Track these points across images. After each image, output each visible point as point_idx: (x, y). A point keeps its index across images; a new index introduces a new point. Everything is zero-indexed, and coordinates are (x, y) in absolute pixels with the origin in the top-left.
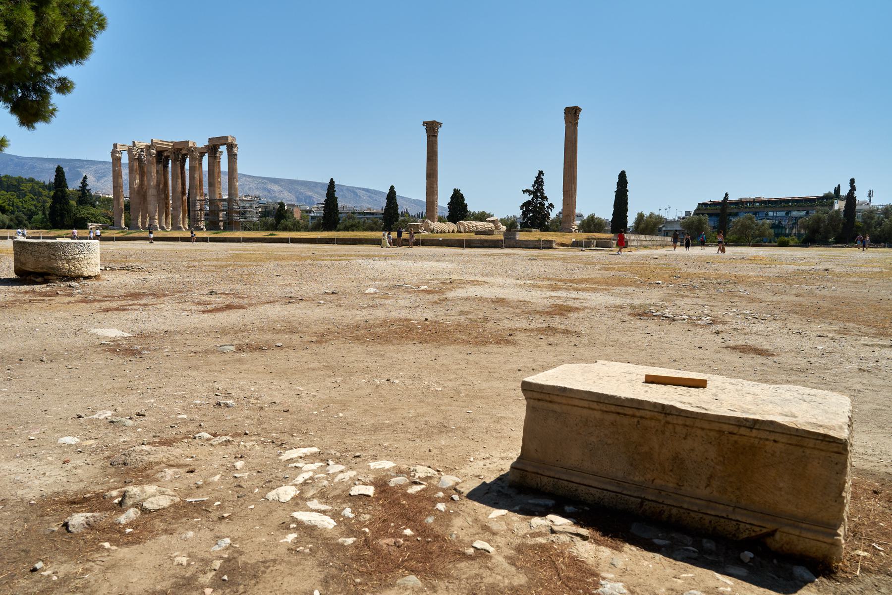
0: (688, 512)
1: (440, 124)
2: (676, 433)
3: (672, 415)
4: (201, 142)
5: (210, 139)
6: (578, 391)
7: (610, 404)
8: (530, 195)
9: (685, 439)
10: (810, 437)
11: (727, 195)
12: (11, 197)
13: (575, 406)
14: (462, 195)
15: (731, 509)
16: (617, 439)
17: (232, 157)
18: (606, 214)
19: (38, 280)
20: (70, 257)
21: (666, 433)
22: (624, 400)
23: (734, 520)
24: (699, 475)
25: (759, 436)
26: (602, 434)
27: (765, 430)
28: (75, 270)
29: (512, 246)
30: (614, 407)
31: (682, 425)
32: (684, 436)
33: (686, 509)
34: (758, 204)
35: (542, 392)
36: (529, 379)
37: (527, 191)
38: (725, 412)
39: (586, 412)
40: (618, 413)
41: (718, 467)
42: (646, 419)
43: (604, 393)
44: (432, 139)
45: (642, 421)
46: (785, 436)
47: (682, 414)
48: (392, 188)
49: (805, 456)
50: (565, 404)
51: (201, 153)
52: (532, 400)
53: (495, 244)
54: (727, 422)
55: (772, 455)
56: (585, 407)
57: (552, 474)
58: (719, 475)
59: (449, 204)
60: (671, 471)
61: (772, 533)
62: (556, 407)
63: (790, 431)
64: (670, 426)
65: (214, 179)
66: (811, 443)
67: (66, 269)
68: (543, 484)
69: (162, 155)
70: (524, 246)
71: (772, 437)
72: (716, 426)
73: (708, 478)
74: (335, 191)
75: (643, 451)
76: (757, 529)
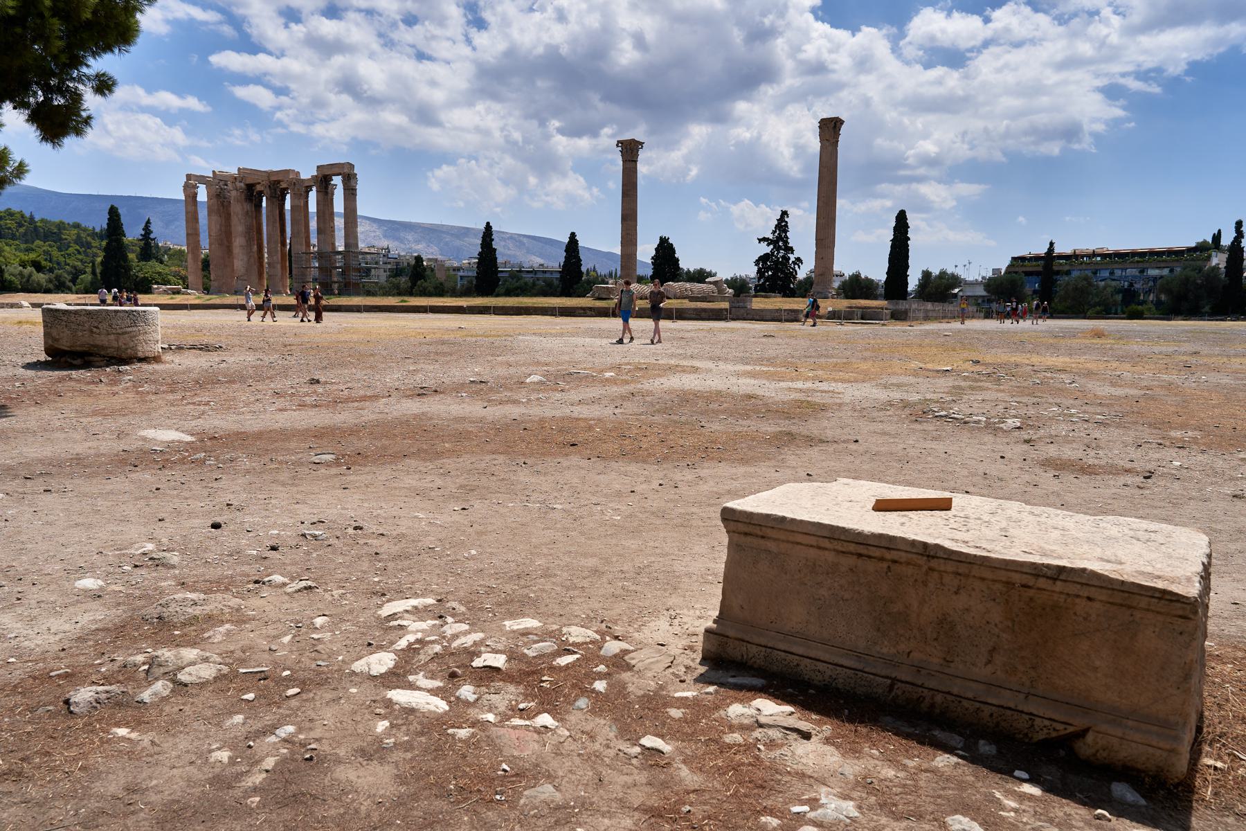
0: (958, 699)
2: (944, 585)
3: (938, 558)
4: (307, 172)
5: (318, 167)
6: (801, 521)
7: (848, 541)
8: (768, 245)
9: (956, 593)
10: (1142, 593)
11: (1052, 244)
12: (50, 249)
13: (798, 543)
15: (1022, 696)
16: (858, 592)
17: (350, 193)
18: (878, 271)
19: (75, 362)
20: (119, 331)
21: (930, 584)
22: (867, 536)
23: (1027, 714)
24: (977, 646)
25: (1065, 592)
26: (836, 584)
27: (1074, 582)
28: (127, 349)
29: (741, 317)
30: (853, 545)
31: (953, 573)
32: (955, 590)
33: (956, 696)
34: (1099, 259)
35: (750, 523)
36: (731, 504)
37: (764, 239)
38: (1017, 554)
39: (813, 553)
40: (860, 555)
41: (1004, 635)
42: (901, 563)
43: (840, 525)
44: (631, 165)
45: (894, 567)
46: (1104, 591)
47: (951, 557)
48: (573, 235)
49: (1133, 621)
50: (783, 541)
51: (307, 187)
52: (736, 535)
53: (717, 315)
54: (1019, 569)
55: (1085, 619)
56: (812, 546)
57: (763, 641)
58: (1006, 647)
59: (653, 258)
60: (936, 639)
61: (1082, 733)
62: (771, 545)
63: (1112, 584)
64: (936, 575)
66: (1144, 602)
67: (112, 347)
68: (751, 655)
69: (253, 191)
70: (758, 317)
71: (1085, 592)
72: (1003, 576)
73: (990, 651)
75: (895, 610)
76: (1060, 727)
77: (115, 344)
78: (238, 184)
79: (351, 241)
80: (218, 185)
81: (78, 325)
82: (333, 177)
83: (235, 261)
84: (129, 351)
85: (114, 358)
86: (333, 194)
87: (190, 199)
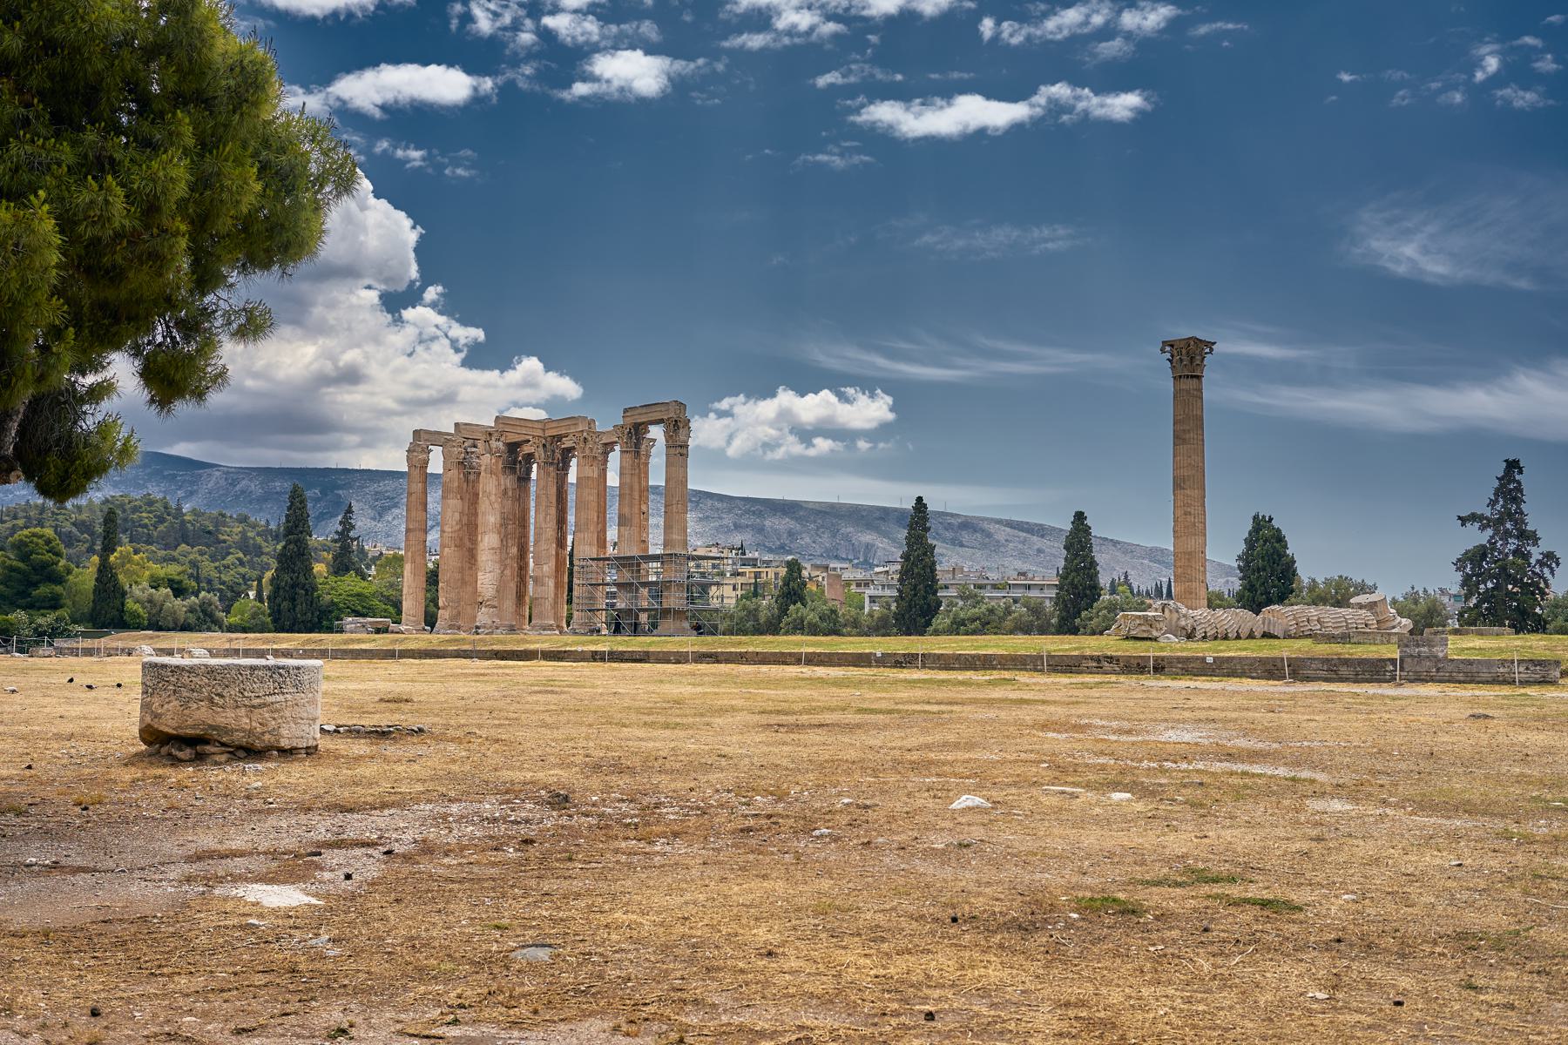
1: (1210, 344)
5: (626, 411)
12: (199, 558)
14: (1278, 530)
17: (678, 449)
19: (180, 754)
20: (256, 702)
28: (263, 734)
37: (1473, 517)
44: (1193, 383)
48: (1080, 517)
51: (606, 444)
53: (1374, 671)
65: (631, 506)
67: (243, 730)
69: (517, 454)
70: (1461, 677)
74: (929, 529)
78: (494, 444)
81: (193, 690)
83: (480, 576)
84: (267, 737)
85: (240, 748)
86: (648, 456)
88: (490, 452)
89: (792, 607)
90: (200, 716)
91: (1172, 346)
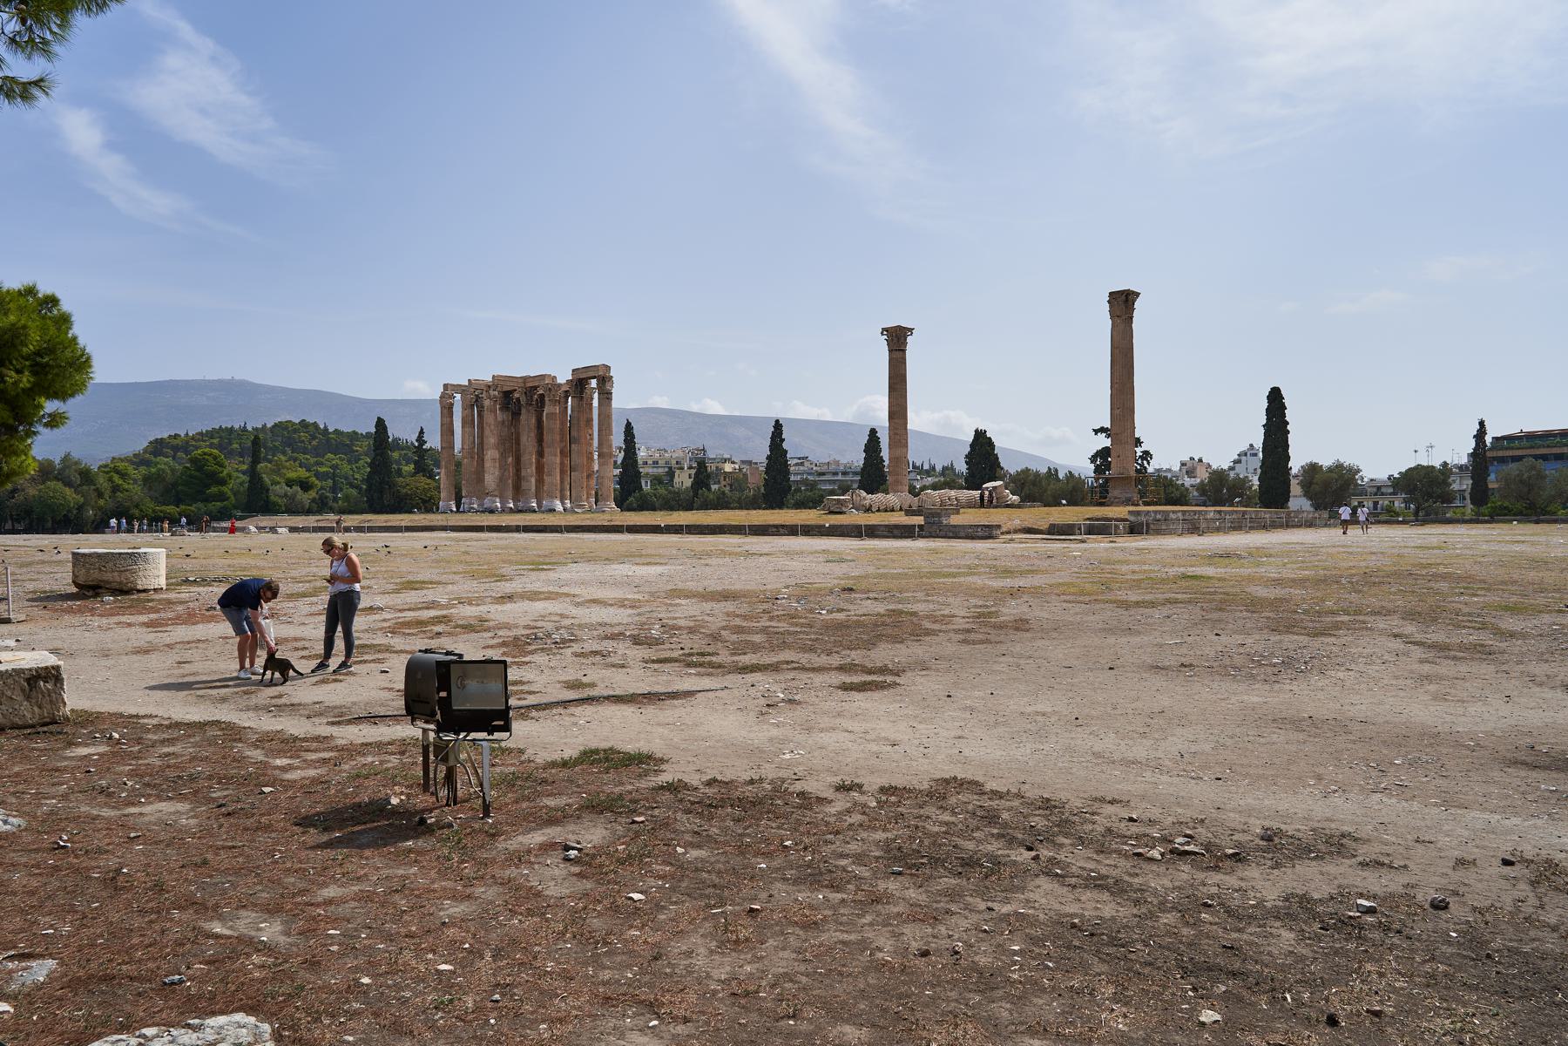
1: (911, 330)
4: (564, 376)
5: (573, 371)
11: (1482, 423)
17: (606, 396)
20: (123, 569)
28: (127, 583)
29: (933, 534)
37: (1102, 430)
44: (899, 354)
53: (906, 532)
70: (951, 535)
77: (118, 579)
79: (605, 450)
80: (475, 395)
82: (592, 380)
85: (116, 590)
87: (445, 411)
88: (490, 398)
89: (700, 491)
90: (95, 575)
91: (887, 331)
